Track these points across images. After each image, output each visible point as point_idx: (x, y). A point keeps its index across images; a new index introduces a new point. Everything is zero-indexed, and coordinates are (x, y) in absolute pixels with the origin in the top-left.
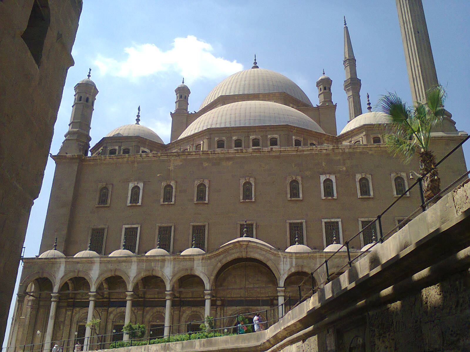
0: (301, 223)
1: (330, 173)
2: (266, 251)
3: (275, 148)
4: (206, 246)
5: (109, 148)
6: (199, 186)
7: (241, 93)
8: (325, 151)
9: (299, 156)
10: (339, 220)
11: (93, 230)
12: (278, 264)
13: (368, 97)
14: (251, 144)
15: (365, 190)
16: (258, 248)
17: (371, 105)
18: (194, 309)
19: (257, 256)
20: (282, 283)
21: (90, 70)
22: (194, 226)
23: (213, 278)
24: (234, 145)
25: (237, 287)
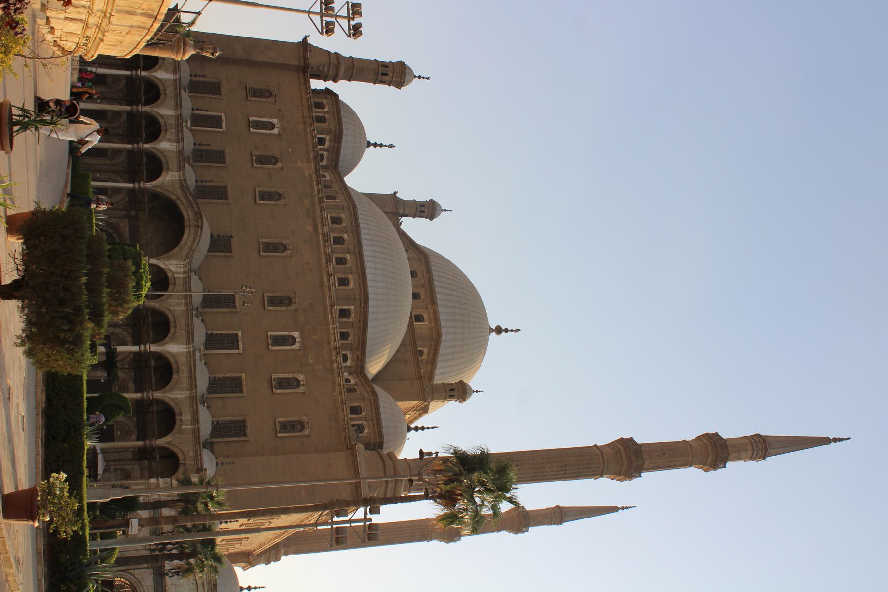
0: (235, 307)
1: (303, 344)
3: (334, 281)
5: (325, 101)
6: (278, 194)
8: (333, 339)
9: (325, 308)
11: (219, 84)
12: (176, 259)
13: (433, 428)
14: (339, 255)
17: (420, 431)
19: (185, 236)
21: (428, 79)
22: (226, 188)
23: (159, 190)
24: (336, 235)
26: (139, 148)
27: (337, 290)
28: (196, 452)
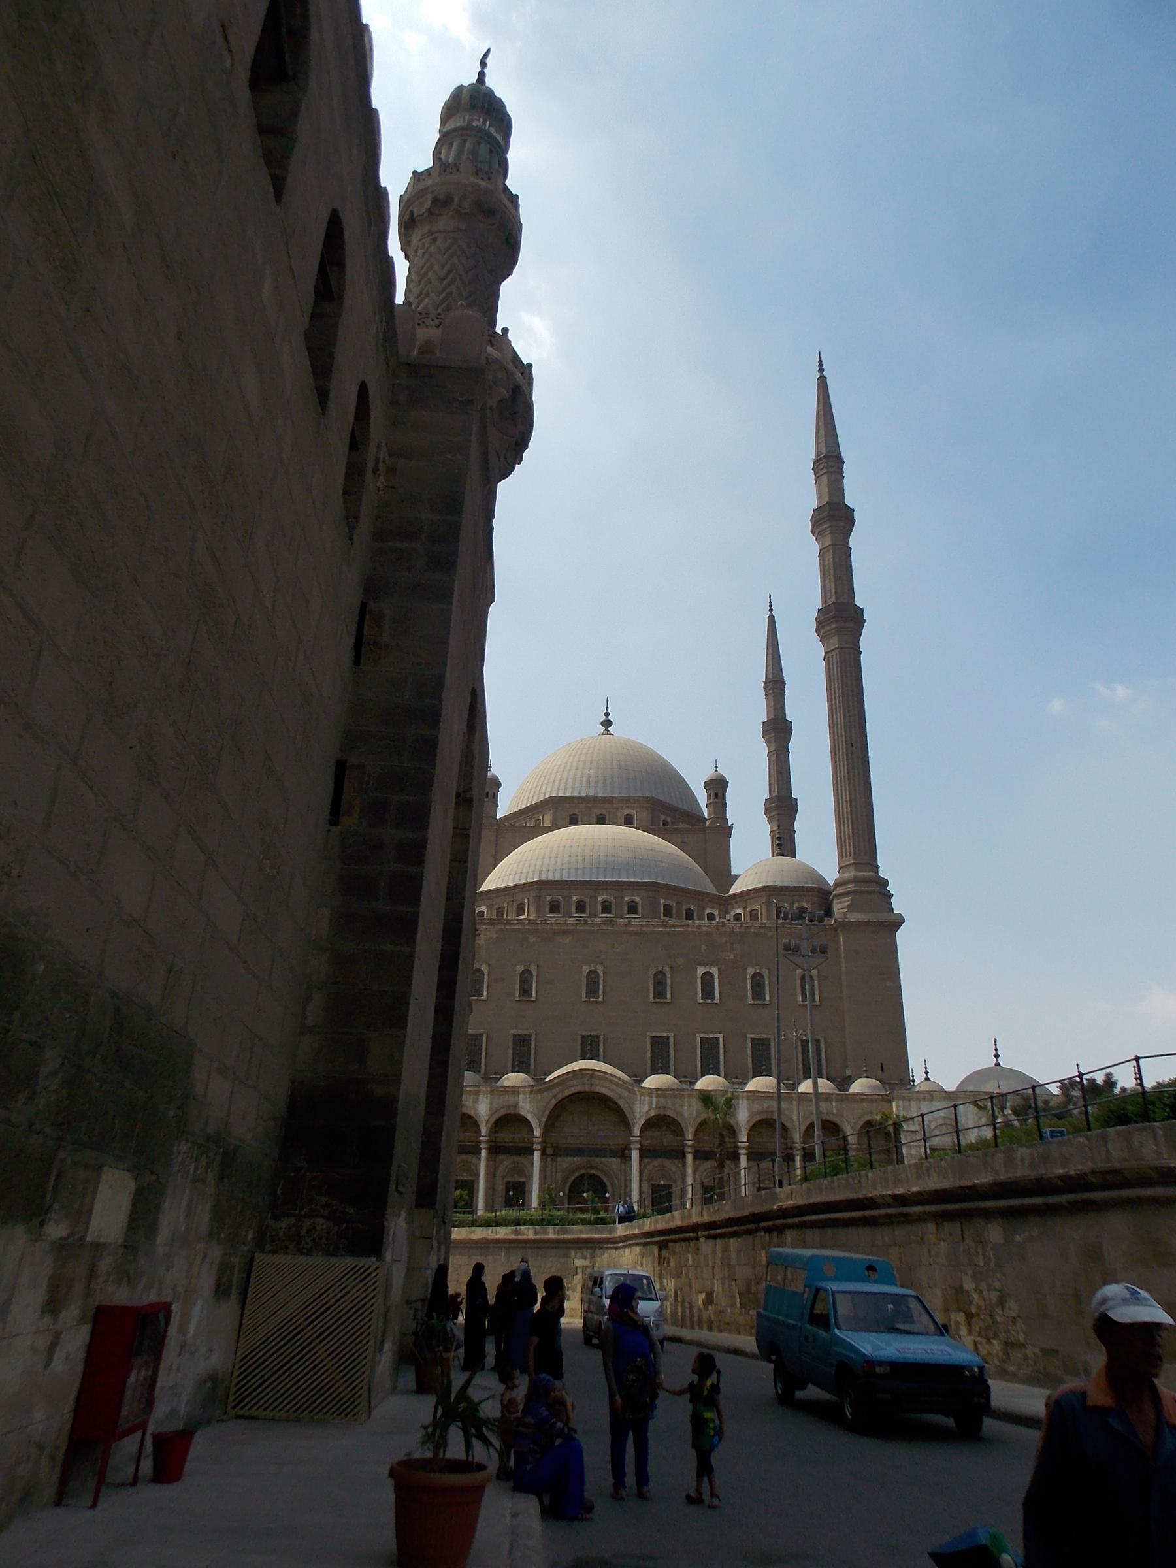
0: (668, 1038)
1: (712, 964)
2: (617, 1084)
4: (532, 1067)
6: (522, 973)
7: (583, 794)
8: (705, 929)
9: (668, 933)
10: (720, 1036)
15: (758, 993)
16: (607, 1079)
18: (516, 1158)
19: (604, 1091)
20: (637, 1132)
22: (514, 1036)
24: (574, 910)
25: (576, 1131)
26: (487, 1142)
27: (643, 917)
28: (862, 1100)
